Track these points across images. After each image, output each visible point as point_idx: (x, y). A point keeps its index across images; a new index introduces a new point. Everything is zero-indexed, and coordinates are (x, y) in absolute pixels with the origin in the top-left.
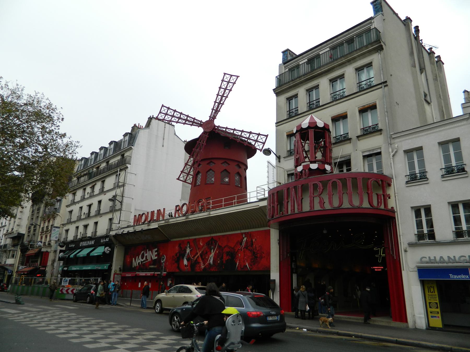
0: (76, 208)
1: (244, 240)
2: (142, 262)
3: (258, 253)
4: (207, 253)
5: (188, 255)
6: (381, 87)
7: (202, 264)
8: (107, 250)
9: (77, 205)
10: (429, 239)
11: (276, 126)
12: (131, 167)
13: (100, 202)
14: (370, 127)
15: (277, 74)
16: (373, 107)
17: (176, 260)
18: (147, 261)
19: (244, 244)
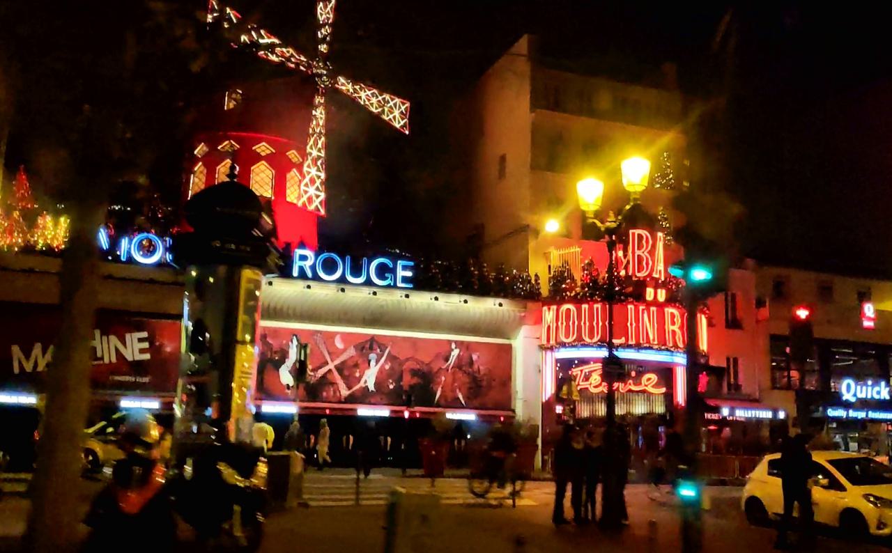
1: (453, 354)
4: (356, 366)
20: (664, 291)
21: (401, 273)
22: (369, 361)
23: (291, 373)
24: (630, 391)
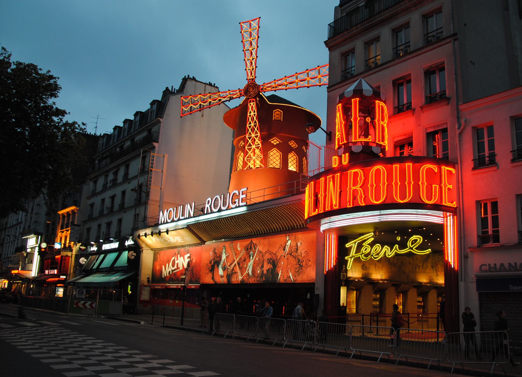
0: (97, 200)
1: (287, 245)
2: (173, 271)
3: (303, 261)
4: (245, 260)
5: (224, 262)
6: (450, 42)
7: (239, 274)
8: (131, 255)
9: (99, 196)
10: (493, 243)
11: (328, 92)
12: (159, 146)
13: (124, 193)
14: (437, 94)
15: (332, 20)
16: (441, 68)
17: (210, 269)
18: (178, 270)
19: (287, 249)
20: (347, 154)
21: (242, 196)
22: (250, 256)
23: (222, 269)
24: (397, 254)
